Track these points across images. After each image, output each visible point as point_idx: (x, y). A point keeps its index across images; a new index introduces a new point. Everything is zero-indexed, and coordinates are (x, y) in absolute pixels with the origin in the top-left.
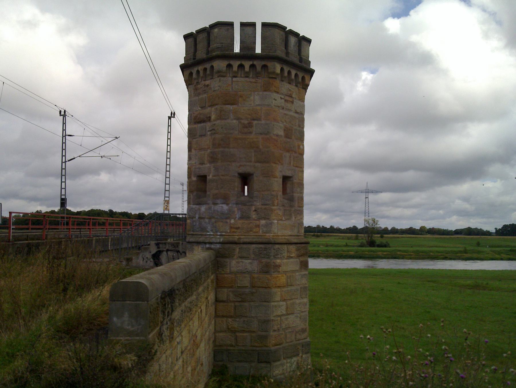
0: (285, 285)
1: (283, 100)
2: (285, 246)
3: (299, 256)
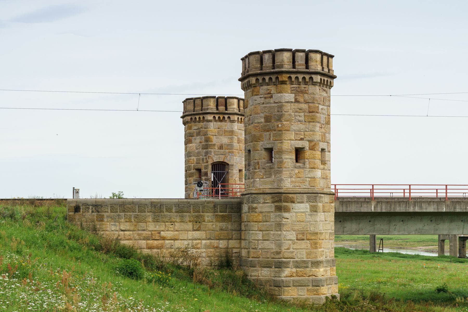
0: (261, 220)
1: (263, 99)
2: (261, 195)
3: (273, 202)
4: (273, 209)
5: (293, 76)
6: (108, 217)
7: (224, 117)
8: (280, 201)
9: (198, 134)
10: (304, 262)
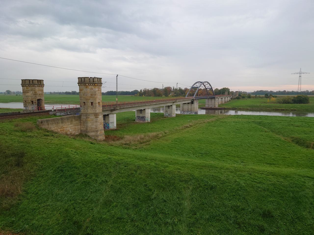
3: (94, 116)
4: (94, 118)
5: (98, 84)
6: (50, 124)
7: (40, 86)
8: (97, 115)
9: (32, 90)
10: (101, 129)
